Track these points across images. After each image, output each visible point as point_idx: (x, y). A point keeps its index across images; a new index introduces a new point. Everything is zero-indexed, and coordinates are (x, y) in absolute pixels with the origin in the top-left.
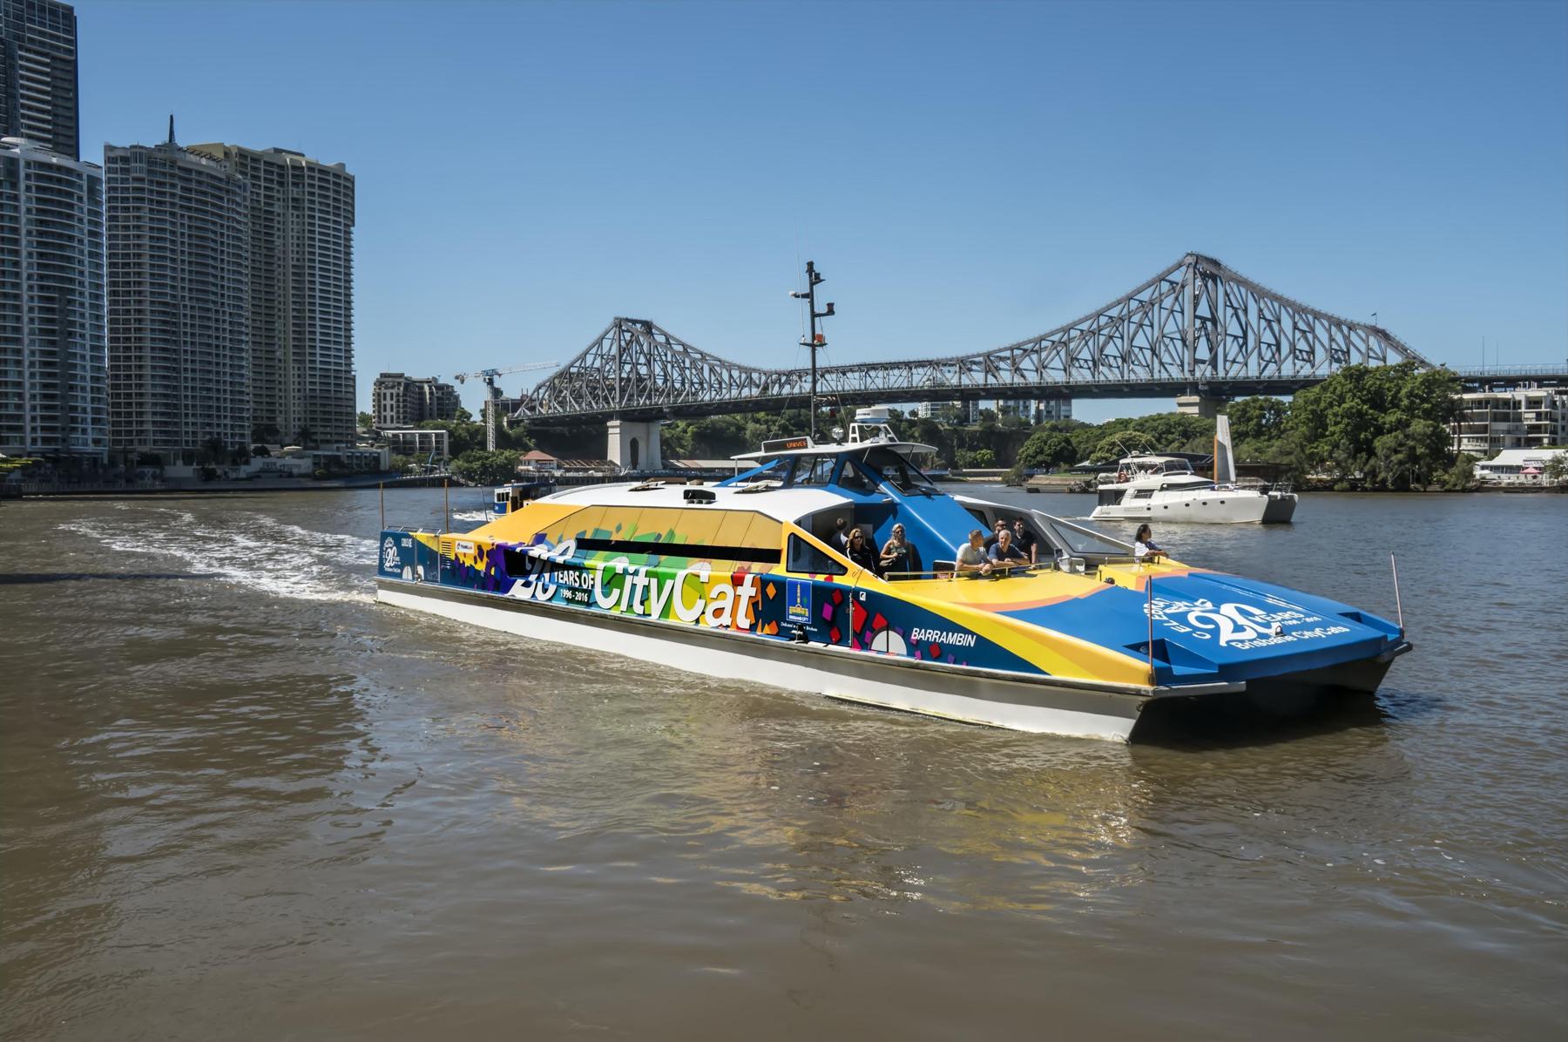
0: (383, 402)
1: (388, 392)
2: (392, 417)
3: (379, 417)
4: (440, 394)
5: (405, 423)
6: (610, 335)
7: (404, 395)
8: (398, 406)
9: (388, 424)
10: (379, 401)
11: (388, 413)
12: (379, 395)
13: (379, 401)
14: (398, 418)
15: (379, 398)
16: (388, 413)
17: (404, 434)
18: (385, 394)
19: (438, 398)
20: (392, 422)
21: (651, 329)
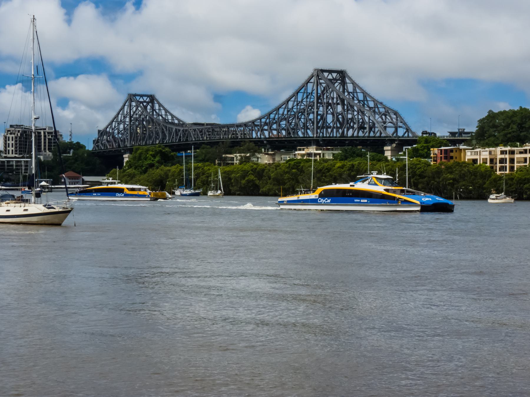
0: (8, 142)
1: (11, 136)
2: (12, 150)
3: (6, 150)
4: (50, 137)
5: (20, 154)
6: (127, 104)
7: (20, 138)
8: (16, 144)
9: (11, 155)
10: (6, 141)
11: (11, 149)
12: (6, 137)
13: (6, 141)
14: (16, 151)
15: (6, 139)
16: (11, 149)
17: (8, 162)
18: (9, 137)
19: (49, 139)
20: (12, 153)
21: (345, 77)
